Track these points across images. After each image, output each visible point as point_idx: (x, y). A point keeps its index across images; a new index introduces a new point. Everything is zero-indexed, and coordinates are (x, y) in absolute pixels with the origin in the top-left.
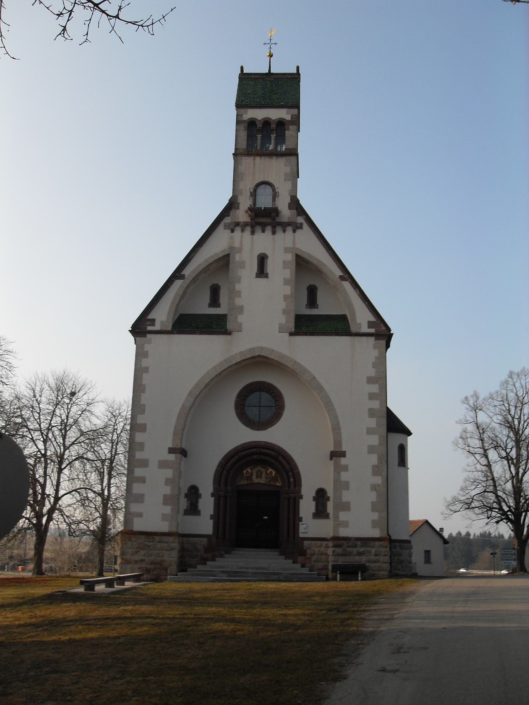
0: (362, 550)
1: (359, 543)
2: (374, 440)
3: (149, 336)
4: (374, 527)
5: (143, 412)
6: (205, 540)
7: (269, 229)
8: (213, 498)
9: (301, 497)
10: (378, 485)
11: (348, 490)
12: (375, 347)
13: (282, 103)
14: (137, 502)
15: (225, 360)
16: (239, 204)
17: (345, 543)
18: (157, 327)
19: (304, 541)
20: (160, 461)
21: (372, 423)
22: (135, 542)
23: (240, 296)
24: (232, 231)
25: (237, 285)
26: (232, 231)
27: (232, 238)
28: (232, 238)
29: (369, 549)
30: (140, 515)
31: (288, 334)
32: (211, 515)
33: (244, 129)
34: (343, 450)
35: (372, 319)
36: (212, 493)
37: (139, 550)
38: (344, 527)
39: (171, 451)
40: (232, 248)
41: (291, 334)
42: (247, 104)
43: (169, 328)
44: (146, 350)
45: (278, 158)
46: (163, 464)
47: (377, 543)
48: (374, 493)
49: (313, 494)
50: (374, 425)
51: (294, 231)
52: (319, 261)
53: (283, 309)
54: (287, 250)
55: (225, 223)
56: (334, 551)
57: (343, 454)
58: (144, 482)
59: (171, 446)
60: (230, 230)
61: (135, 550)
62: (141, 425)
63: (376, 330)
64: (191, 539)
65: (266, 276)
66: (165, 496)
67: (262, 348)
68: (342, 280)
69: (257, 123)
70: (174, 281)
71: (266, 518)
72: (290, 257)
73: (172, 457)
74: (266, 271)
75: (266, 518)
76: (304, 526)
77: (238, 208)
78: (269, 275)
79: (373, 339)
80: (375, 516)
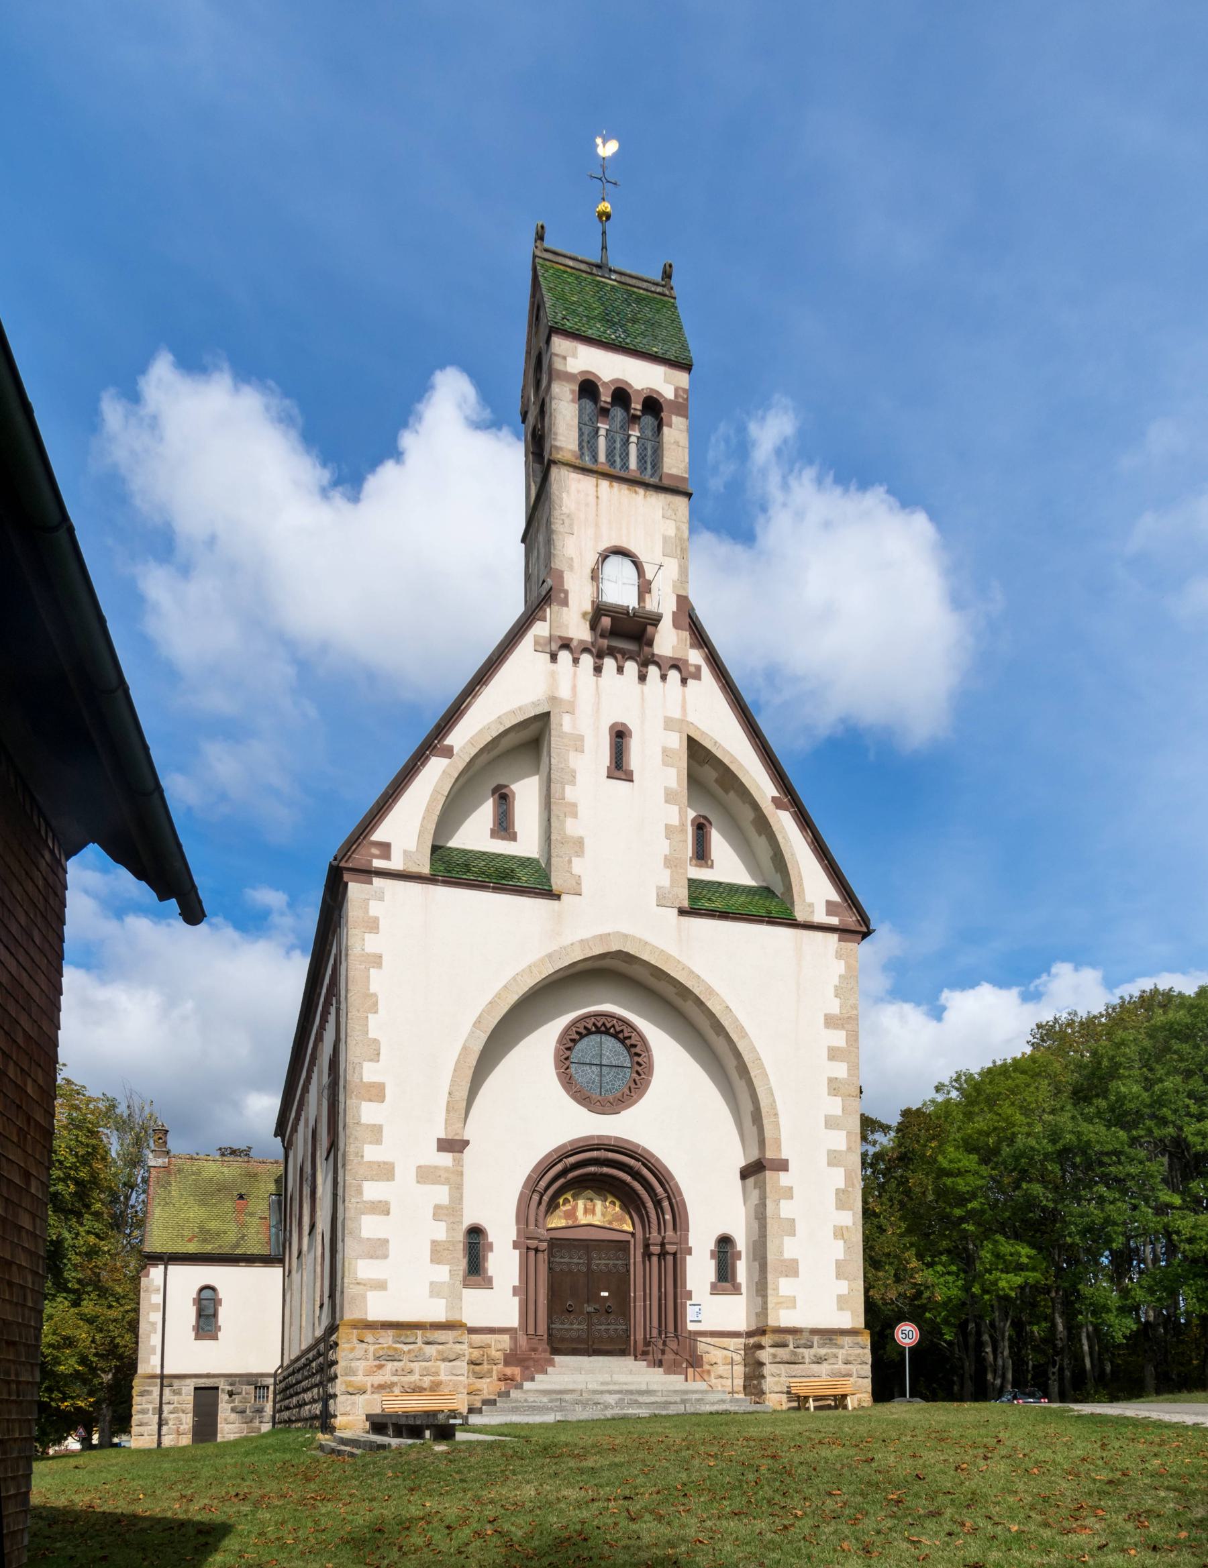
0: (823, 1351)
1: (816, 1338)
3: (377, 881)
4: (840, 1309)
5: (377, 1056)
6: (506, 1338)
8: (517, 1252)
14: (371, 1258)
15: (550, 956)
17: (790, 1339)
22: (374, 1344)
23: (575, 815)
25: (568, 788)
29: (834, 1350)
30: (381, 1286)
32: (514, 1287)
34: (783, 1157)
36: (514, 1241)
38: (787, 1308)
43: (426, 870)
44: (372, 913)
47: (847, 1340)
48: (841, 1242)
49: (712, 1245)
51: (684, 681)
54: (669, 724)
57: (783, 1166)
58: (387, 1213)
59: (443, 1136)
61: (377, 1363)
62: (373, 1085)
66: (434, 1243)
70: (428, 758)
71: (606, 1294)
72: (677, 743)
74: (628, 764)
75: (606, 1294)
78: (635, 777)
80: (843, 1287)
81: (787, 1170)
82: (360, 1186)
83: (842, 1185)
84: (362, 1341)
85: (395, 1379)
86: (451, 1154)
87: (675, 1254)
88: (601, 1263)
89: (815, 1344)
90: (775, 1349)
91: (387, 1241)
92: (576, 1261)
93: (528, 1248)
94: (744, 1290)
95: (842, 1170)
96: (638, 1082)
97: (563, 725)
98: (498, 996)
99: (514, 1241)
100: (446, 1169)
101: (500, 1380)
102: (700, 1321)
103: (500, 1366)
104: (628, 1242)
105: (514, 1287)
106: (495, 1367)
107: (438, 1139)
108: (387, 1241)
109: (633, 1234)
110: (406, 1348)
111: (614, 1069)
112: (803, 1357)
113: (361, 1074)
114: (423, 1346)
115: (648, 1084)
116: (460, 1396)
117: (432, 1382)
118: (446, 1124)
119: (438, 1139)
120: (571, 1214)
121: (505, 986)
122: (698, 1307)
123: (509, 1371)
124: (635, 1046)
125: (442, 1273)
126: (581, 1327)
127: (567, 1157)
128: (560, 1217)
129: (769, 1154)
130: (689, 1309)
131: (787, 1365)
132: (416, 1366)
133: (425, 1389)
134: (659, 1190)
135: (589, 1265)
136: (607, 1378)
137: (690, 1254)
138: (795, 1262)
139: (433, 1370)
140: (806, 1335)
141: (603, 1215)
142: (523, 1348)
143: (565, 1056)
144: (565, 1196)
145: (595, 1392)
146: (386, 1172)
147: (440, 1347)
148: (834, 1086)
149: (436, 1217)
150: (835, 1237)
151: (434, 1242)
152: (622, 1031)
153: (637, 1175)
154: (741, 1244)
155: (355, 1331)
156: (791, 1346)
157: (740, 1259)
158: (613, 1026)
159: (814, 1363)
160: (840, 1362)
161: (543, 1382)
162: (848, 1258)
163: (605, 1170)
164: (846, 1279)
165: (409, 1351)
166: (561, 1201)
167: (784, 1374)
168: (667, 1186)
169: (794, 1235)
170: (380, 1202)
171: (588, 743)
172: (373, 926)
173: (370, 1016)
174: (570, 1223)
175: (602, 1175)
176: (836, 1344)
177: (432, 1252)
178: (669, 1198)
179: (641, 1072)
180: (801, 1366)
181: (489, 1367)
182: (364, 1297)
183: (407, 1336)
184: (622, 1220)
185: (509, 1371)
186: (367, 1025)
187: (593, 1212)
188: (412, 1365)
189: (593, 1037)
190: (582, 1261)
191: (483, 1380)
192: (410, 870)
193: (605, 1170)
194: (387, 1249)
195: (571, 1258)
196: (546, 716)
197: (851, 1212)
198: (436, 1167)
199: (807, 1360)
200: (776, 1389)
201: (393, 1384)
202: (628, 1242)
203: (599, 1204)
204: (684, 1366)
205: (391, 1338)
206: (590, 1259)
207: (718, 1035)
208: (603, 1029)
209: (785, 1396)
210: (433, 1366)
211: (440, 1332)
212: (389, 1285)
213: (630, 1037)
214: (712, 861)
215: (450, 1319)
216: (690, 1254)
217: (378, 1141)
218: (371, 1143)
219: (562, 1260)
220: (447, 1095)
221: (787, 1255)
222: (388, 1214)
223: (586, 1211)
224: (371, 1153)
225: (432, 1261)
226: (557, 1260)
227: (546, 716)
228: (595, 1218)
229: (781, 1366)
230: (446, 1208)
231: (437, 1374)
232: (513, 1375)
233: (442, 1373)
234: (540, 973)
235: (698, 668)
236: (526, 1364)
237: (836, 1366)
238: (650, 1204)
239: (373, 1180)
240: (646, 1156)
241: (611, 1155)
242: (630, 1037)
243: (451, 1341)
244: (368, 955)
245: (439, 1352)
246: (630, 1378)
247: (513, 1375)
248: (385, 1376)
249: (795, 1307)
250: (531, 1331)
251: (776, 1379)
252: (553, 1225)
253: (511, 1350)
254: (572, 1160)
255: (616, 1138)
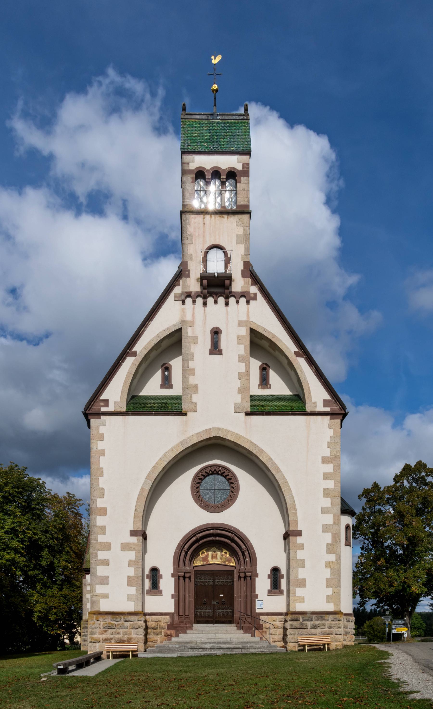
0: (317, 623)
1: (314, 617)
2: (329, 519)
4: (328, 602)
5: (103, 496)
6: (168, 617)
7: (221, 300)
8: (174, 578)
9: (257, 576)
10: (332, 562)
11: (304, 567)
12: (330, 427)
13: (232, 149)
14: (102, 584)
15: (182, 442)
16: (189, 271)
17: (300, 617)
18: (111, 408)
19: (261, 617)
20: (122, 544)
21: (327, 502)
22: (103, 621)
23: (194, 374)
24: (184, 302)
25: (190, 362)
26: (184, 302)
27: (183, 310)
28: (183, 310)
29: (323, 622)
30: (106, 596)
31: (244, 414)
32: (172, 595)
33: (191, 180)
35: (327, 397)
36: (172, 574)
37: (107, 629)
38: (300, 602)
39: (133, 533)
40: (183, 322)
41: (247, 414)
42: (194, 149)
43: (124, 409)
44: (101, 432)
45: (229, 216)
46: (125, 547)
47: (331, 617)
48: (329, 570)
50: (329, 505)
51: (248, 302)
52: (274, 336)
53: (239, 388)
54: (240, 324)
55: (175, 293)
56: (292, 625)
57: (299, 533)
59: (132, 529)
60: (181, 302)
61: (104, 629)
63: (331, 409)
64: (155, 618)
65: (220, 353)
67: (218, 429)
68: (297, 356)
69: (206, 174)
71: (222, 595)
72: (244, 332)
73: (134, 540)
74: (220, 347)
75: (222, 595)
76: (261, 602)
77: (188, 276)
78: (223, 352)
79: (328, 417)
81: (301, 536)
82: (96, 553)
83: (330, 541)
84: (98, 620)
85: (112, 636)
86: (136, 537)
87: (251, 577)
88: (220, 581)
89: (314, 619)
90: (292, 622)
91: (108, 577)
92: (208, 581)
93: (179, 577)
94: (285, 593)
95: (330, 534)
96: (232, 496)
97: (188, 333)
98: (157, 463)
99: (172, 574)
100: (134, 544)
101: (165, 636)
102: (262, 608)
103: (166, 630)
104: (233, 571)
105: (172, 595)
106: (163, 630)
107: (130, 531)
108: (108, 577)
109: (235, 567)
110: (116, 623)
111: (221, 490)
112: (306, 626)
113: (96, 504)
114: (124, 622)
115: (237, 496)
116: (140, 644)
117: (128, 638)
118: (134, 524)
119: (130, 531)
120: (205, 559)
121: (161, 458)
122: (262, 602)
123: (169, 632)
124: (231, 479)
125: (133, 590)
126: (210, 611)
127: (197, 534)
128: (200, 561)
129: (291, 529)
130: (257, 602)
131: (298, 630)
132: (121, 631)
133: (125, 641)
134: (243, 547)
135: (214, 582)
136: (213, 635)
137: (257, 577)
138: (304, 580)
139: (129, 633)
140: (309, 615)
141: (221, 559)
142: (177, 622)
143: (196, 487)
144: (202, 551)
145: (203, 643)
146: (107, 546)
147: (132, 623)
148: (327, 493)
149: (130, 566)
150: (326, 567)
151: (129, 577)
152: (224, 472)
153: (233, 540)
154: (283, 571)
155: (95, 616)
156: (301, 621)
157: (283, 578)
158: (220, 470)
159: (312, 628)
160: (326, 628)
161: (183, 637)
162: (332, 577)
163: (218, 538)
164: (331, 587)
165: (118, 625)
166: (201, 553)
167: (297, 634)
168: (246, 545)
169: (304, 567)
170: (105, 560)
171: (200, 340)
172: (101, 437)
173: (100, 477)
174: (205, 563)
175: (216, 540)
176: (324, 619)
177: (128, 581)
178: (248, 550)
179: (233, 491)
180: (306, 630)
181: (160, 630)
182: (99, 601)
183: (116, 618)
184: (230, 561)
185: (169, 632)
186: (99, 482)
187: (216, 557)
188: (119, 630)
189: (211, 476)
190: (210, 581)
191: (158, 636)
192: (117, 410)
193: (218, 538)
194: (108, 581)
195: (205, 579)
196: (180, 330)
197: (335, 555)
198: (129, 543)
199: (309, 627)
200: (292, 641)
201: (111, 639)
202: (233, 571)
203: (219, 553)
204: (253, 629)
205: (110, 619)
206: (214, 579)
207: (269, 472)
208: (215, 472)
209: (297, 644)
210: (128, 631)
211: (131, 616)
212: (109, 596)
213: (228, 475)
214: (270, 385)
215: (137, 610)
216: (257, 577)
217: (104, 533)
218: (101, 534)
219: (201, 581)
220: (134, 510)
221: (300, 576)
222: (109, 565)
223: (213, 557)
224: (101, 538)
225: (128, 585)
226: (199, 580)
227: (180, 330)
228: (217, 560)
229: (295, 630)
230: (134, 561)
231: (130, 634)
232: (171, 634)
233: (133, 634)
234: (177, 451)
235: (255, 294)
236: (178, 629)
237: (324, 630)
238: (240, 553)
239: (102, 550)
240: (236, 532)
241: (219, 532)
242: (228, 475)
243: (136, 620)
244: (99, 450)
245: (131, 625)
246: (224, 636)
247: (171, 634)
248: (108, 635)
249: (304, 602)
250: (181, 614)
251: (293, 636)
252: (197, 565)
253: (170, 623)
254: (200, 535)
255: (221, 524)
